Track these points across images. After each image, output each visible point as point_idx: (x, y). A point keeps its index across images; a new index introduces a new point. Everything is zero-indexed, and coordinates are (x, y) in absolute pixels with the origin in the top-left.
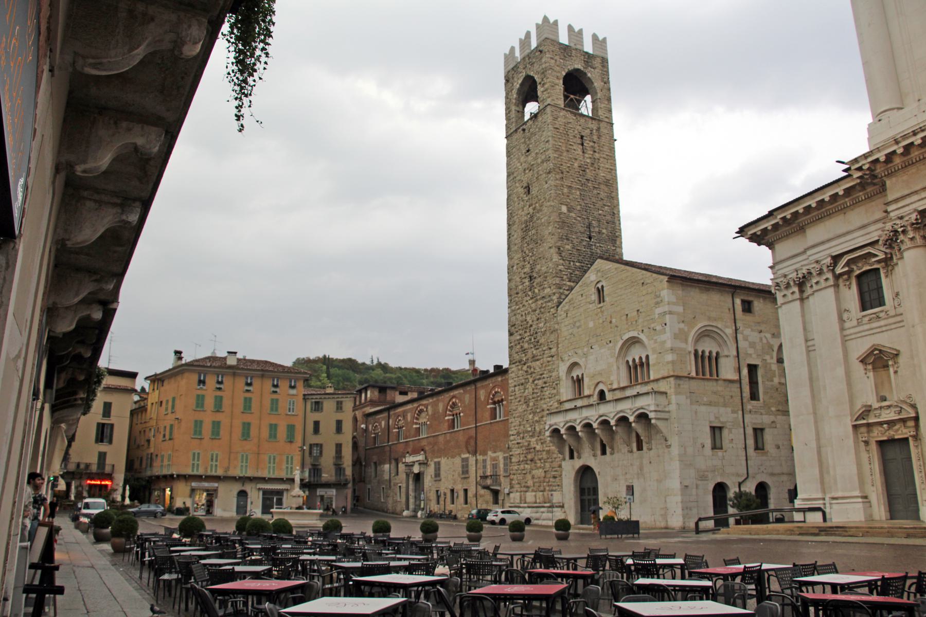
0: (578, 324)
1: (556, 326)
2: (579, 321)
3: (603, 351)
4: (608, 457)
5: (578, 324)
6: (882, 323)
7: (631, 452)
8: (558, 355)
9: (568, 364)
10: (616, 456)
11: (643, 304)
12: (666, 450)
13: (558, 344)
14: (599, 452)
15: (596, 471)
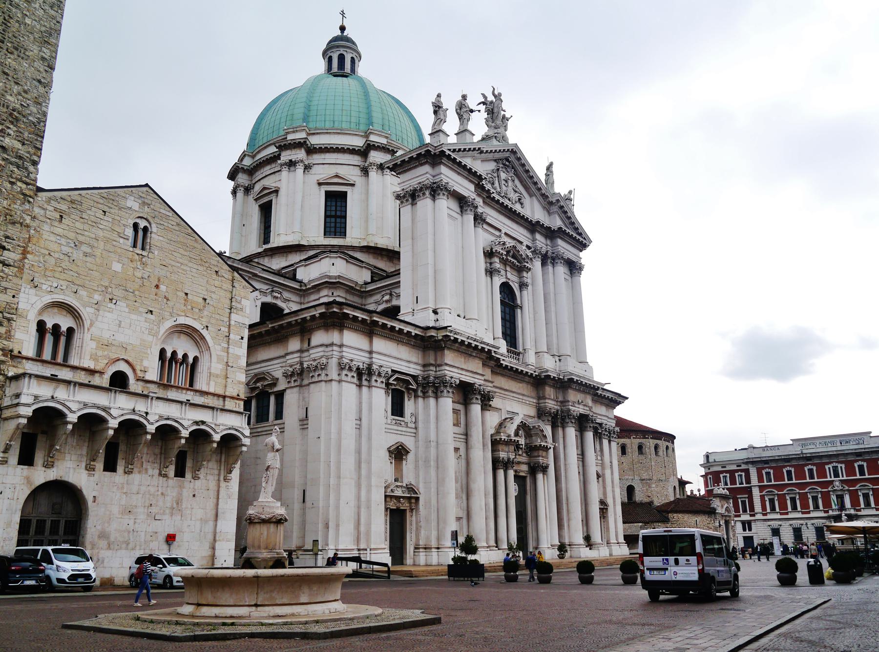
0: (85, 248)
1: (28, 220)
2: (92, 247)
3: (134, 317)
4: (119, 476)
5: (85, 248)
6: (400, 428)
7: (165, 476)
8: (21, 269)
9: (48, 299)
10: (136, 477)
11: (213, 295)
12: (223, 484)
13: (25, 253)
14: (100, 465)
15: (88, 494)
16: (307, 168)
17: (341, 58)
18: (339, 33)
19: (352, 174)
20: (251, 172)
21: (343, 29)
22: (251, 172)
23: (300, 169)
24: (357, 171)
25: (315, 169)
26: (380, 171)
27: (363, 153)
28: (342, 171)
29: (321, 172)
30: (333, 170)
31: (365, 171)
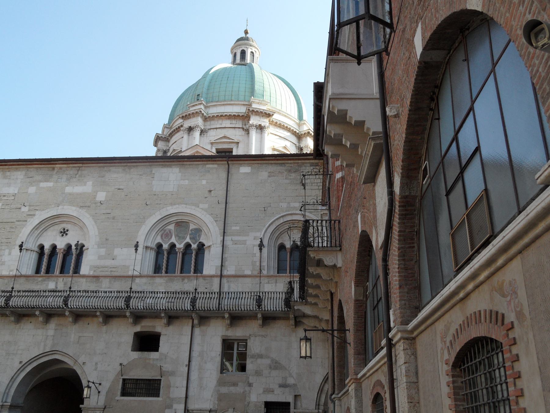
16: (202, 132)
17: (243, 53)
18: (244, 35)
19: (236, 135)
20: (167, 139)
21: (246, 32)
22: (167, 139)
23: (197, 134)
24: (243, 133)
25: (212, 133)
26: (259, 131)
27: (245, 118)
28: (231, 133)
29: (213, 135)
30: (221, 133)
31: (247, 131)
